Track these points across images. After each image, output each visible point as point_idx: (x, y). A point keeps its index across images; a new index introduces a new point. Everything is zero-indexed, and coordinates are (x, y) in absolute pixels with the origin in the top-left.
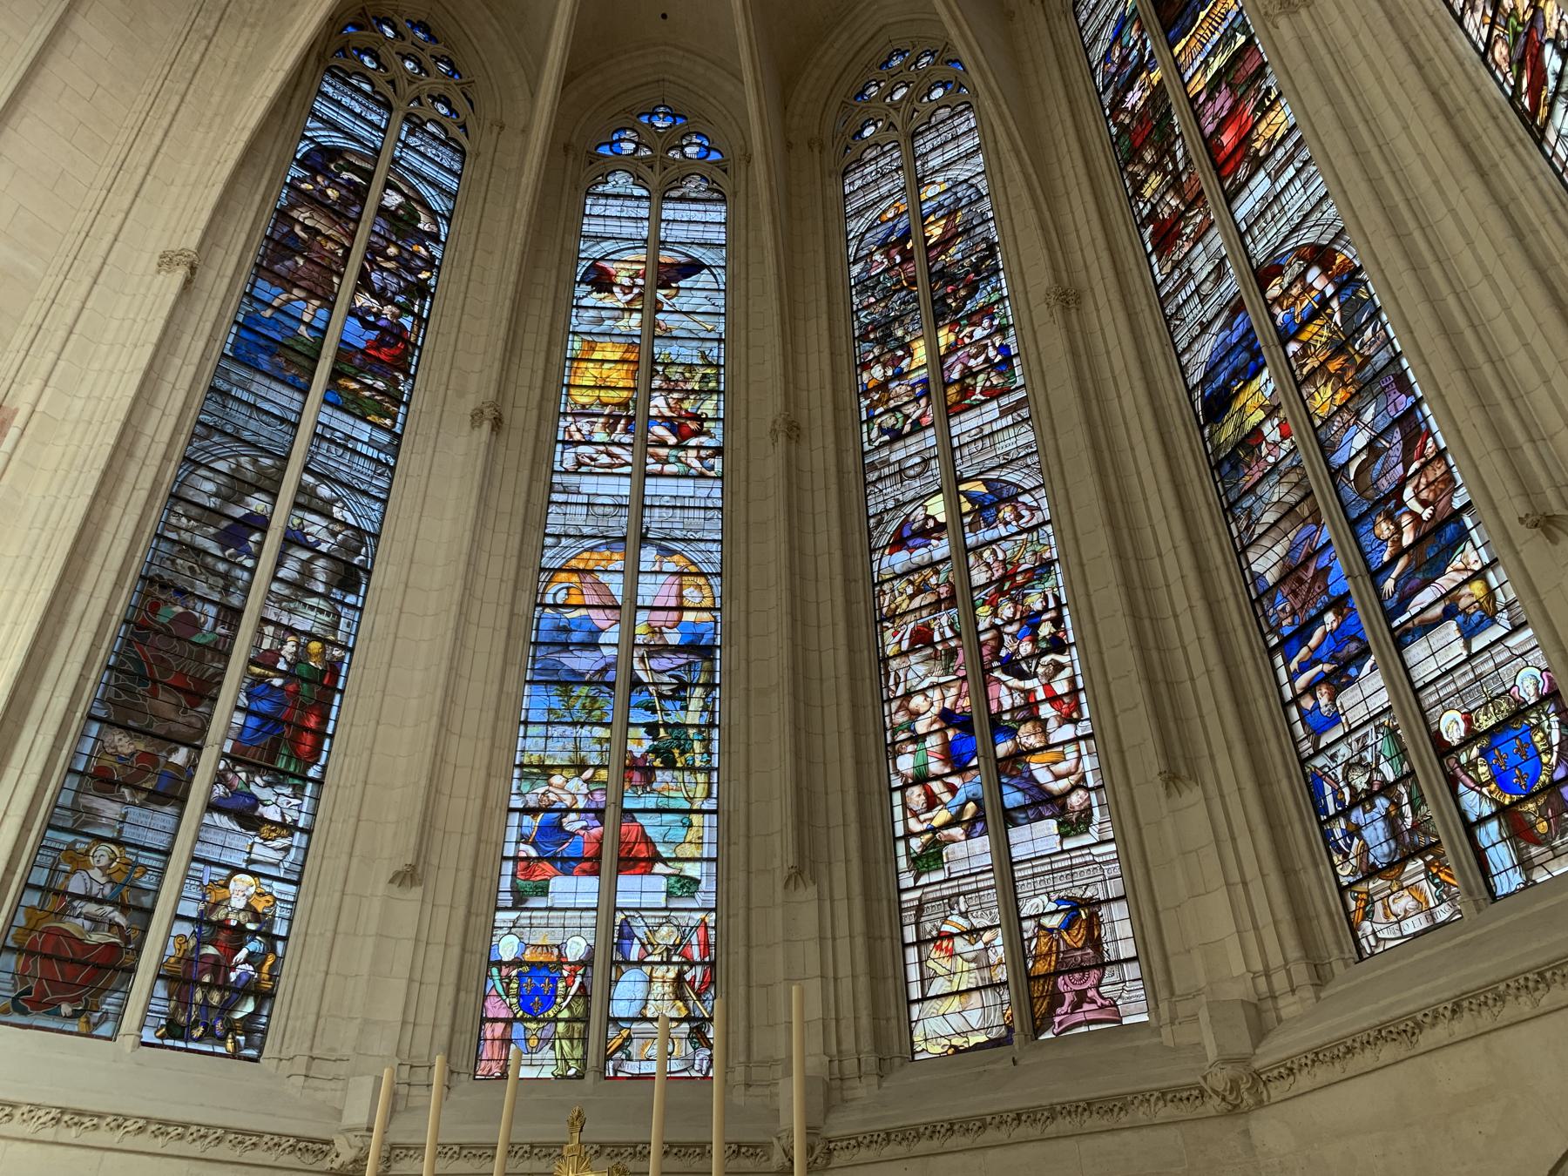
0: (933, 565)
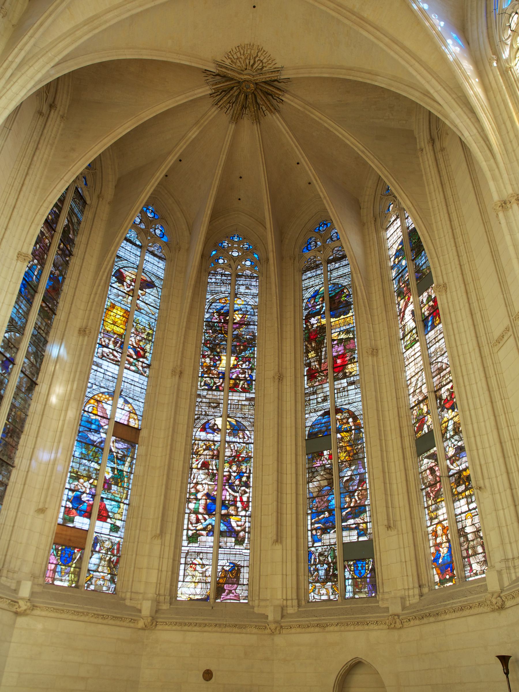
0: (213, 441)
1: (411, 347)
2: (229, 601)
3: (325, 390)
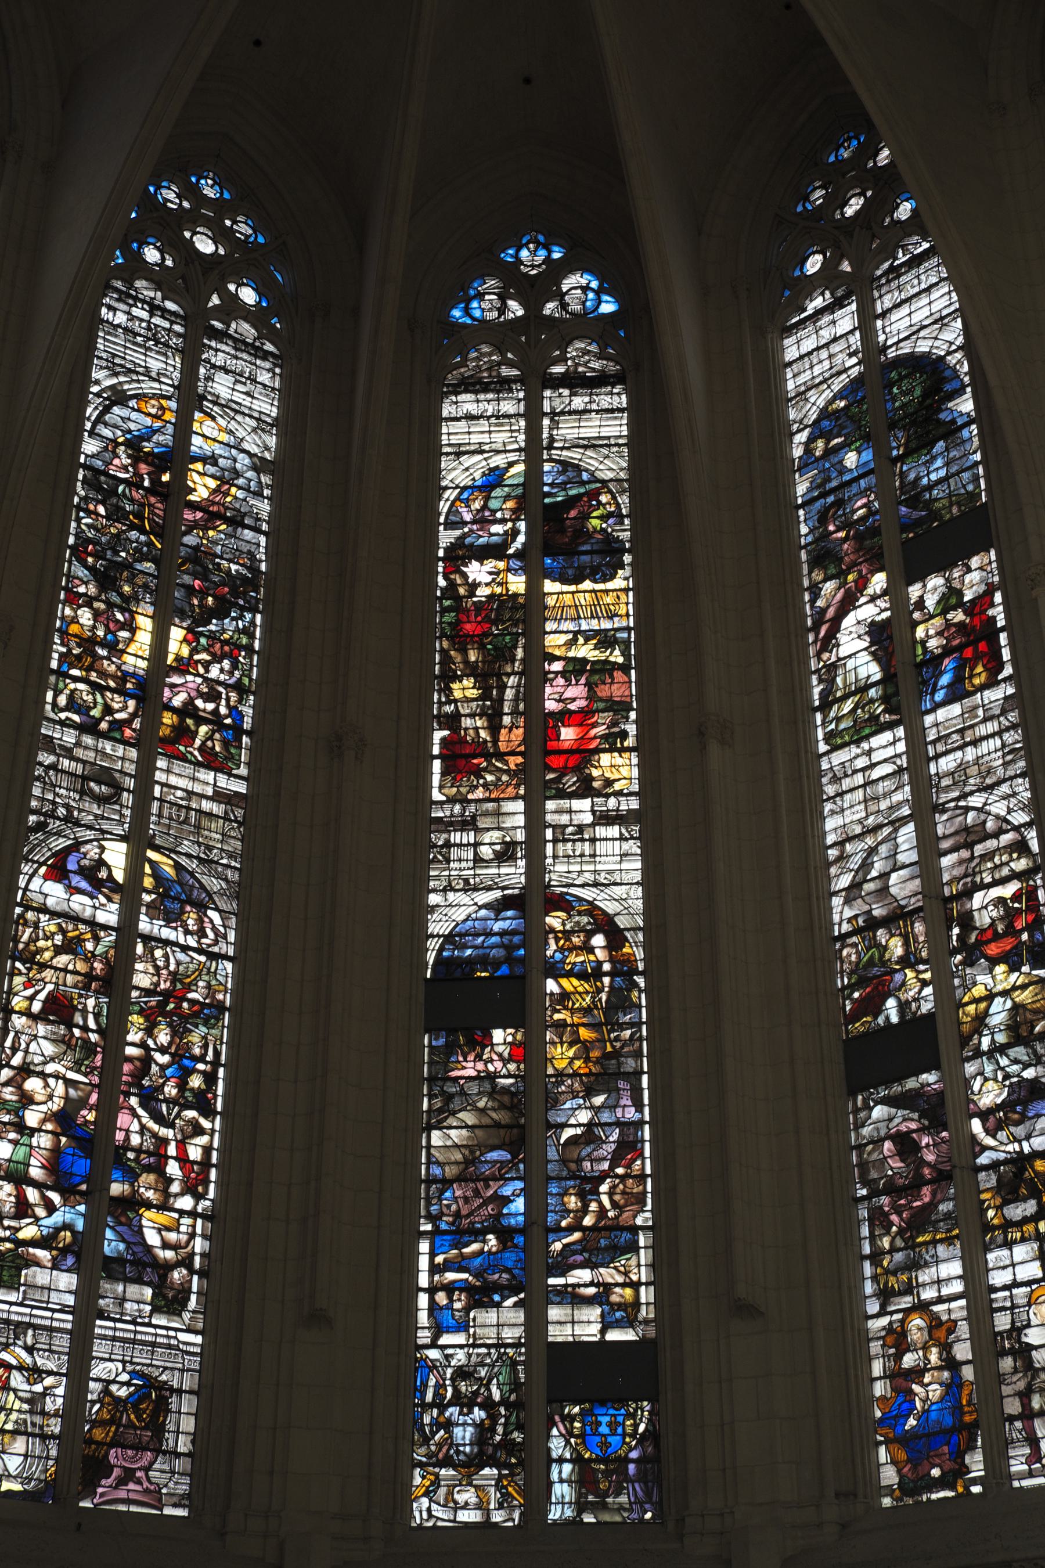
1: (857, 742)
2: (123, 1508)
3: (508, 823)
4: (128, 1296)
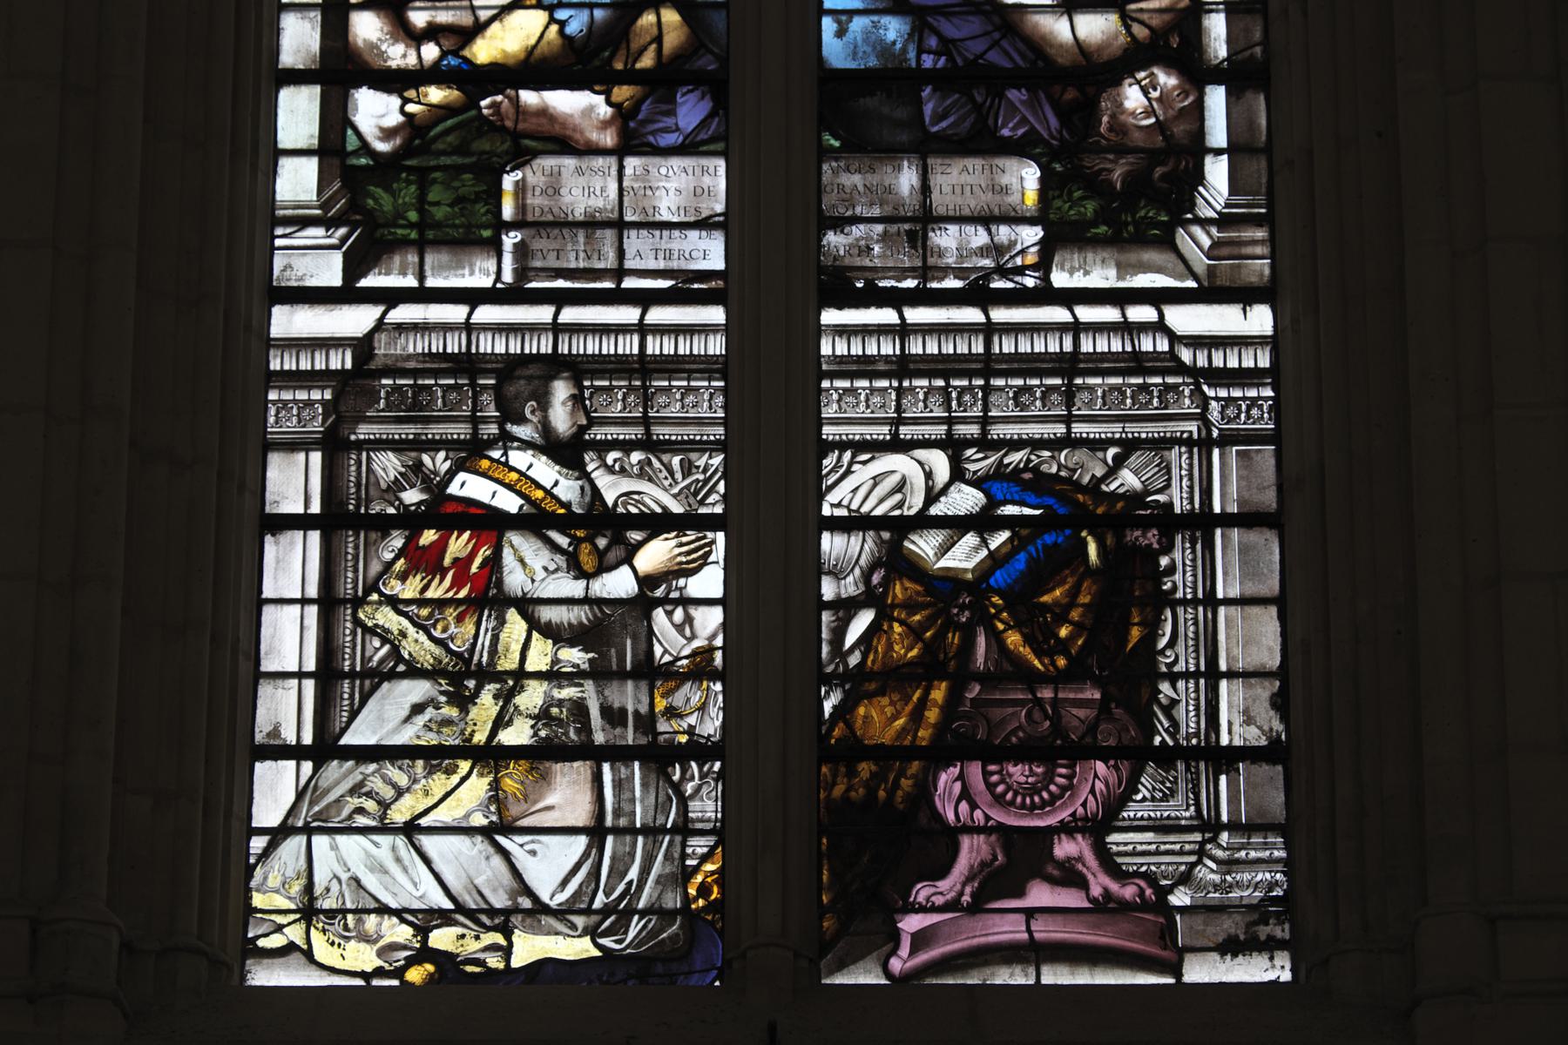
4: (941, 201)
